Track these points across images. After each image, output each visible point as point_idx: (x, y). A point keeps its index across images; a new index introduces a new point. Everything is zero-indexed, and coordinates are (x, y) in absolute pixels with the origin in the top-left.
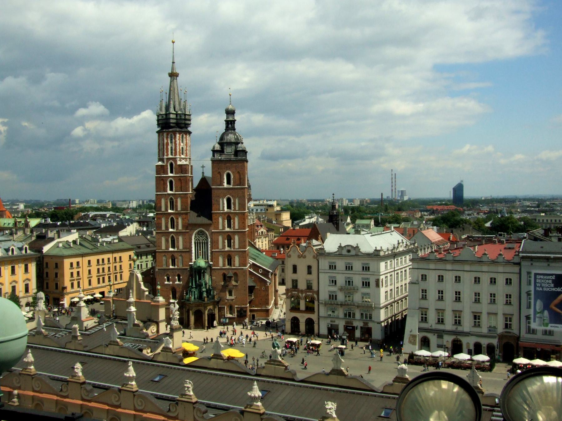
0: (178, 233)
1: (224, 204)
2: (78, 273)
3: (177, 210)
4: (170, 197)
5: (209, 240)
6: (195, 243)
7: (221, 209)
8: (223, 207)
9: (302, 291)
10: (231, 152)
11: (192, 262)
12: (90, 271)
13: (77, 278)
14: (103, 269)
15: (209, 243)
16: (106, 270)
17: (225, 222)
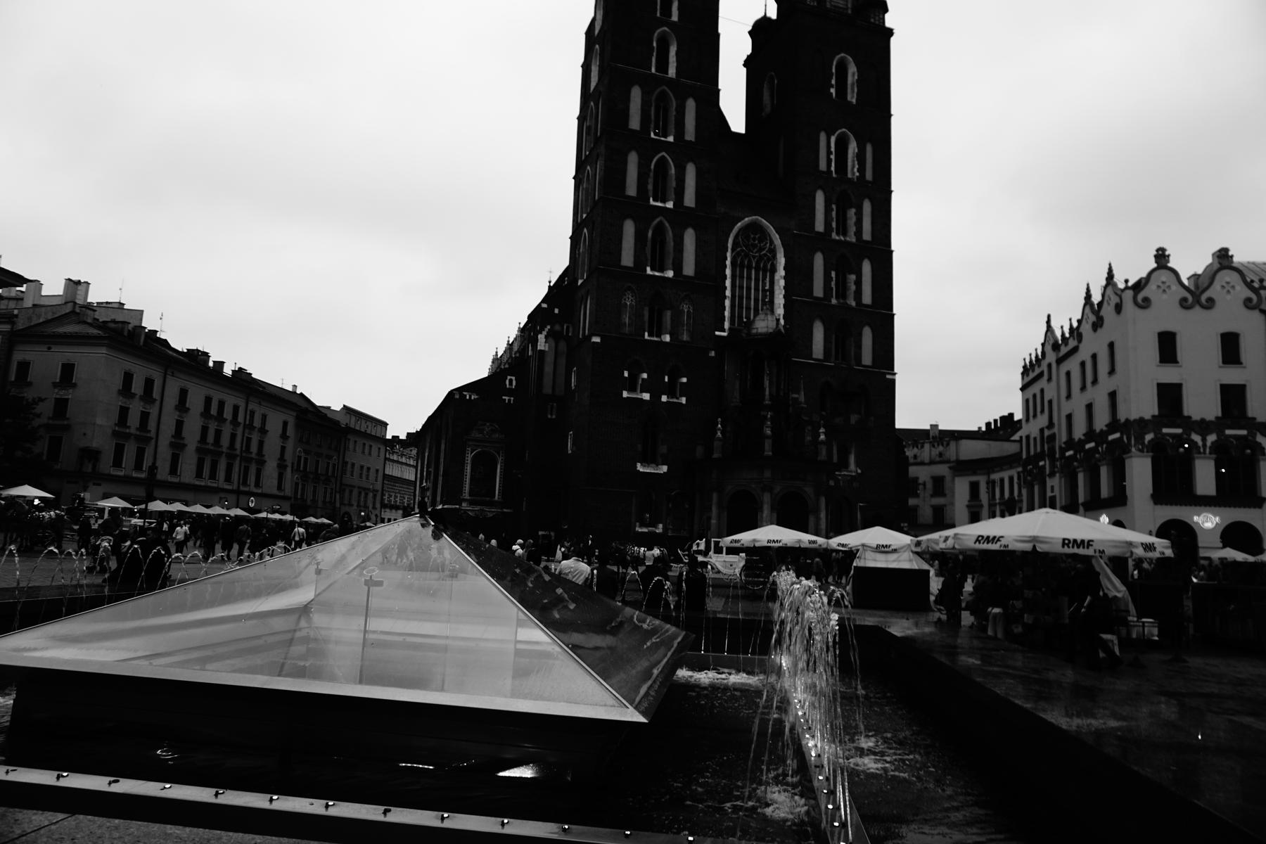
0: (681, 217)
1: (831, 153)
2: (145, 416)
3: (680, 133)
4: (658, 90)
5: (781, 261)
6: (733, 263)
7: (823, 166)
8: (829, 161)
9: (1204, 427)
10: (845, 7)
11: (724, 331)
12: (179, 425)
13: (138, 433)
14: (218, 433)
15: (781, 272)
16: (225, 441)
17: (832, 210)
